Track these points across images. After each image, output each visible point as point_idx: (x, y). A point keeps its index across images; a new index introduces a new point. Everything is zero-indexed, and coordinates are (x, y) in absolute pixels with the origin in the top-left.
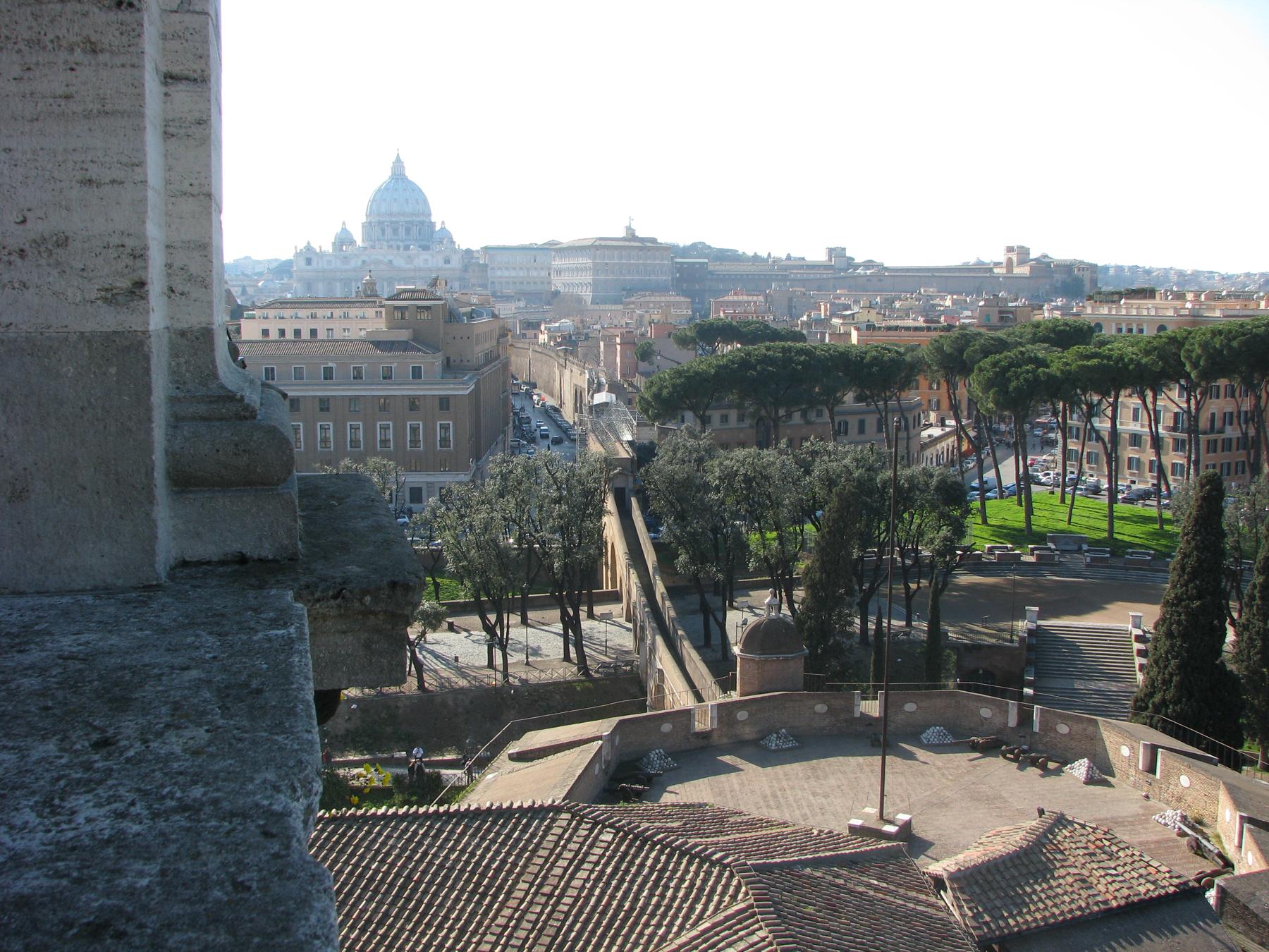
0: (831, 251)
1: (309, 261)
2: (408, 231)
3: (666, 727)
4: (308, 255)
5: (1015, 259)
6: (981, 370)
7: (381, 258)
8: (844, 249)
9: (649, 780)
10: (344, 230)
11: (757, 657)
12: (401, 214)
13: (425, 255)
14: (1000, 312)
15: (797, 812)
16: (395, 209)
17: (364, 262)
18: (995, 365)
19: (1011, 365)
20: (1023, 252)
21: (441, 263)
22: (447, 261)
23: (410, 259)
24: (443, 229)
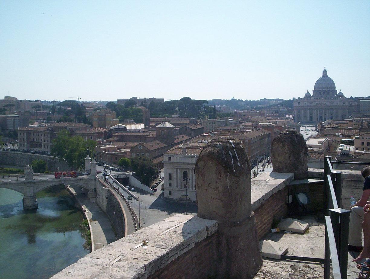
1: (299, 103)
2: (328, 93)
7: (322, 102)
17: (317, 103)
23: (332, 103)
24: (340, 93)
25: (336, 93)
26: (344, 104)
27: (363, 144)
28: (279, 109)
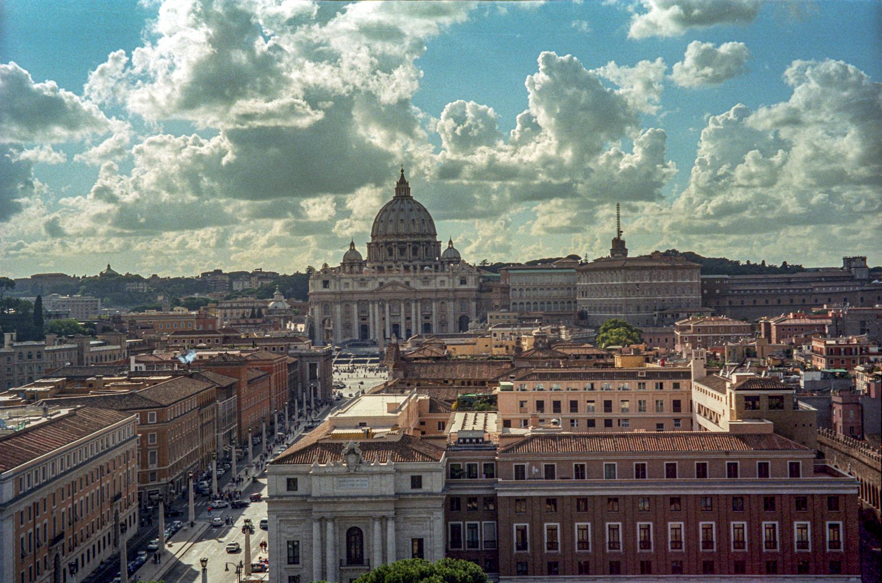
0: (847, 261)
1: (326, 284)
7: (397, 280)
8: (864, 259)
16: (402, 229)
17: (381, 284)
22: (463, 282)
23: (426, 280)
24: (451, 248)
26: (461, 283)
28: (263, 305)
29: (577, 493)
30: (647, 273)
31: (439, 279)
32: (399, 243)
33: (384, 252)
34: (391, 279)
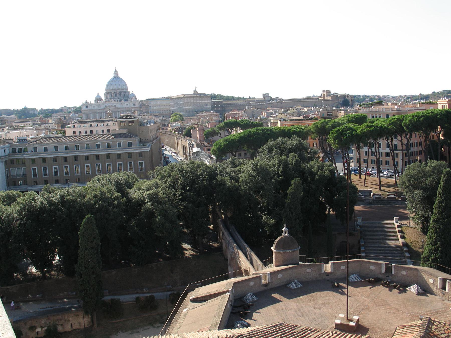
0: (264, 95)
1: (87, 107)
2: (120, 95)
3: (252, 284)
4: (87, 105)
5: (326, 94)
6: (332, 133)
7: (112, 105)
8: (268, 94)
9: (248, 307)
10: (98, 96)
11: (281, 252)
12: (117, 90)
13: (127, 103)
14: (328, 113)
15: (311, 317)
16: (115, 87)
17: (106, 106)
18: (337, 131)
19: (343, 131)
20: (328, 92)
21: (132, 106)
22: (134, 105)
24: (132, 94)
25: (129, 95)
27: (74, 133)
29: (52, 156)
30: (192, 99)
31: (126, 104)
32: (115, 92)
33: (109, 96)
34: (109, 104)
